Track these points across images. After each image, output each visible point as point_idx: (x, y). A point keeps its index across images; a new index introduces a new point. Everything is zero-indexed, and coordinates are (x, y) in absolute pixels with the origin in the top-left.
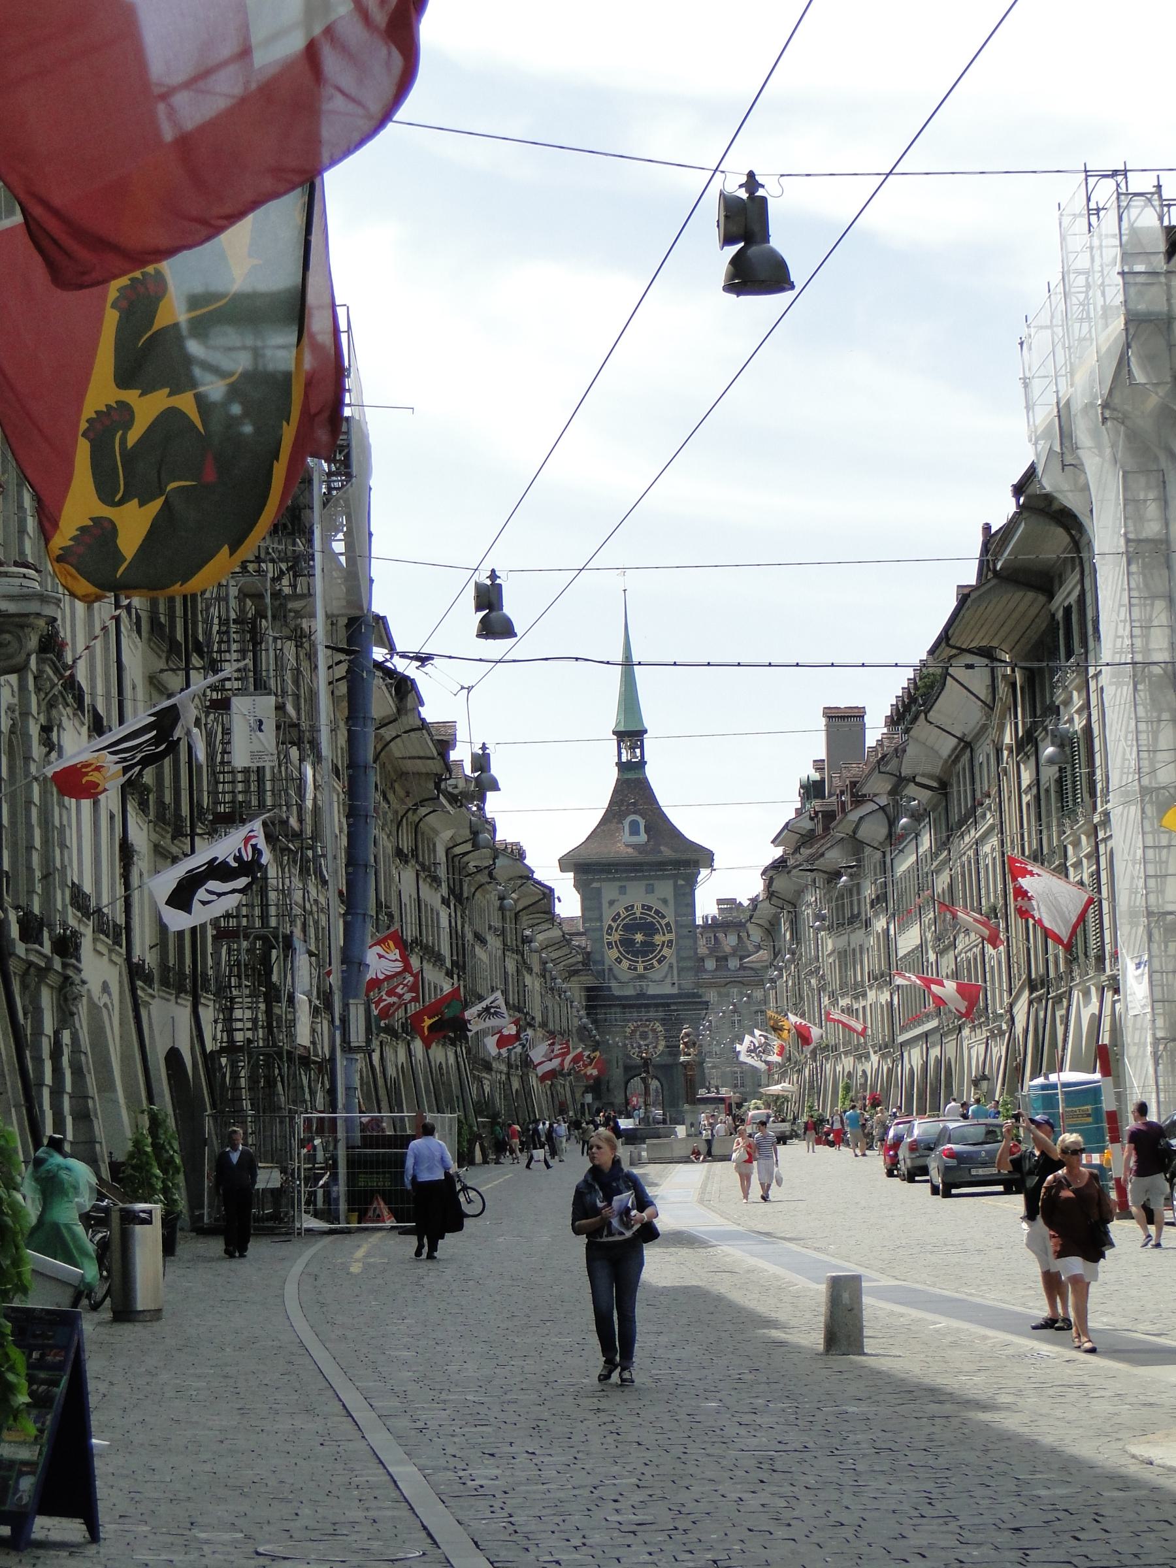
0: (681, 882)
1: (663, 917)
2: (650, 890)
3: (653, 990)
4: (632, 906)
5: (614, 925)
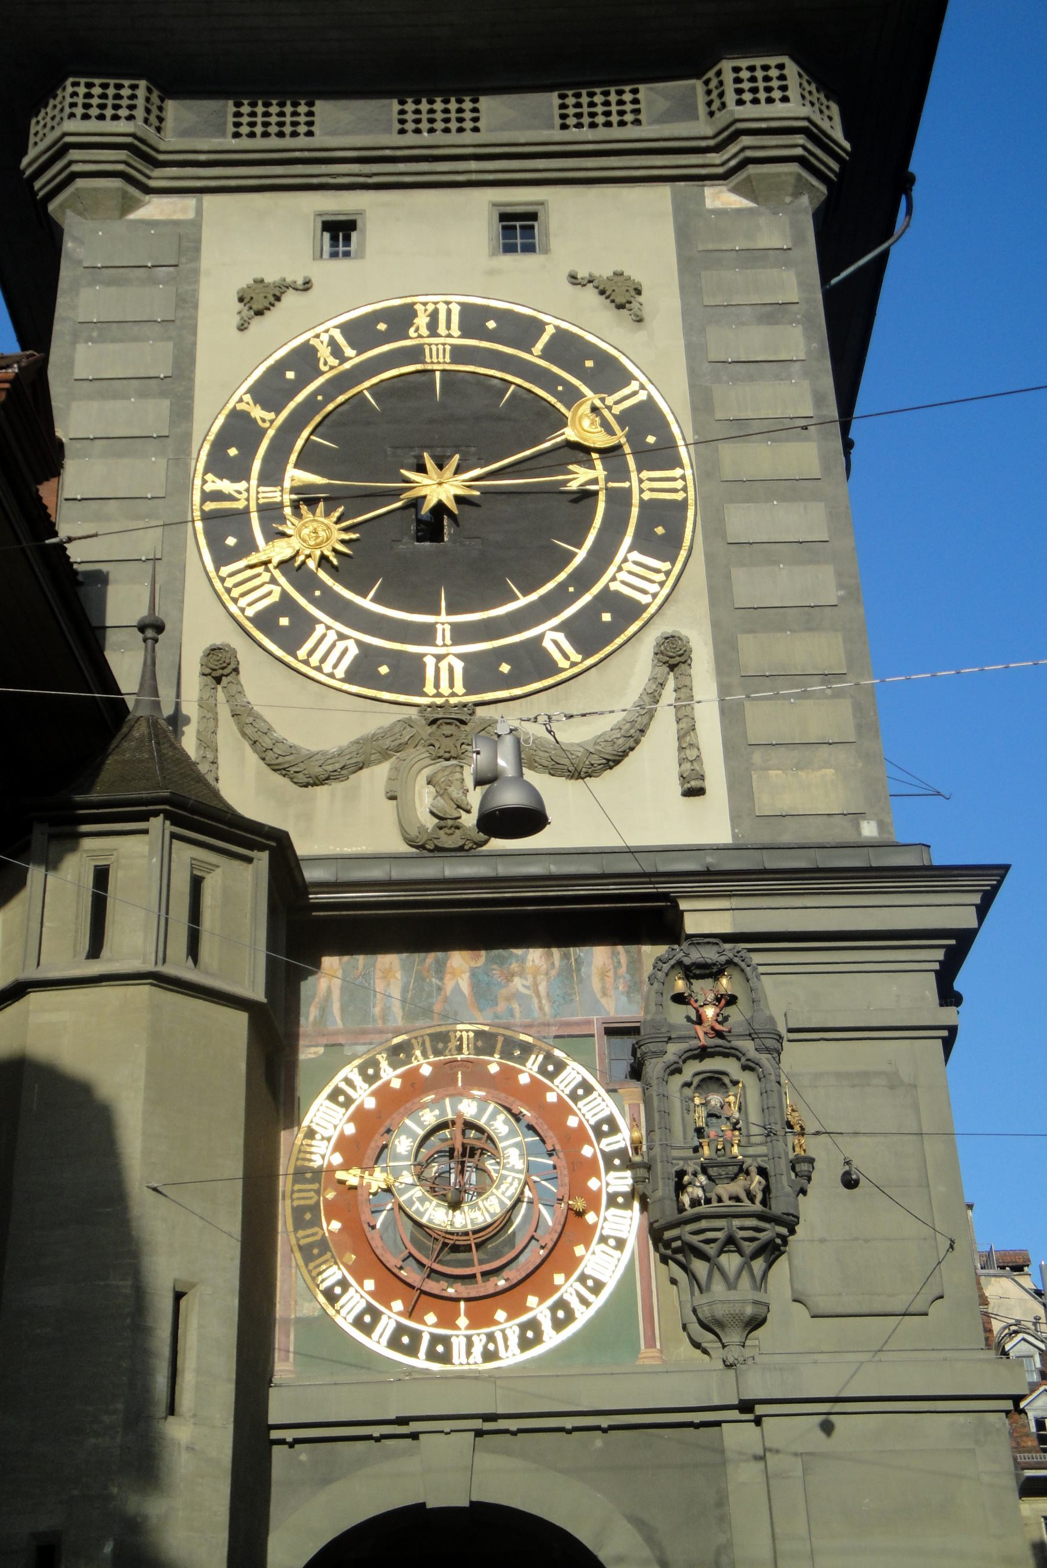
0: (720, 198)
4: (401, 319)
5: (270, 421)
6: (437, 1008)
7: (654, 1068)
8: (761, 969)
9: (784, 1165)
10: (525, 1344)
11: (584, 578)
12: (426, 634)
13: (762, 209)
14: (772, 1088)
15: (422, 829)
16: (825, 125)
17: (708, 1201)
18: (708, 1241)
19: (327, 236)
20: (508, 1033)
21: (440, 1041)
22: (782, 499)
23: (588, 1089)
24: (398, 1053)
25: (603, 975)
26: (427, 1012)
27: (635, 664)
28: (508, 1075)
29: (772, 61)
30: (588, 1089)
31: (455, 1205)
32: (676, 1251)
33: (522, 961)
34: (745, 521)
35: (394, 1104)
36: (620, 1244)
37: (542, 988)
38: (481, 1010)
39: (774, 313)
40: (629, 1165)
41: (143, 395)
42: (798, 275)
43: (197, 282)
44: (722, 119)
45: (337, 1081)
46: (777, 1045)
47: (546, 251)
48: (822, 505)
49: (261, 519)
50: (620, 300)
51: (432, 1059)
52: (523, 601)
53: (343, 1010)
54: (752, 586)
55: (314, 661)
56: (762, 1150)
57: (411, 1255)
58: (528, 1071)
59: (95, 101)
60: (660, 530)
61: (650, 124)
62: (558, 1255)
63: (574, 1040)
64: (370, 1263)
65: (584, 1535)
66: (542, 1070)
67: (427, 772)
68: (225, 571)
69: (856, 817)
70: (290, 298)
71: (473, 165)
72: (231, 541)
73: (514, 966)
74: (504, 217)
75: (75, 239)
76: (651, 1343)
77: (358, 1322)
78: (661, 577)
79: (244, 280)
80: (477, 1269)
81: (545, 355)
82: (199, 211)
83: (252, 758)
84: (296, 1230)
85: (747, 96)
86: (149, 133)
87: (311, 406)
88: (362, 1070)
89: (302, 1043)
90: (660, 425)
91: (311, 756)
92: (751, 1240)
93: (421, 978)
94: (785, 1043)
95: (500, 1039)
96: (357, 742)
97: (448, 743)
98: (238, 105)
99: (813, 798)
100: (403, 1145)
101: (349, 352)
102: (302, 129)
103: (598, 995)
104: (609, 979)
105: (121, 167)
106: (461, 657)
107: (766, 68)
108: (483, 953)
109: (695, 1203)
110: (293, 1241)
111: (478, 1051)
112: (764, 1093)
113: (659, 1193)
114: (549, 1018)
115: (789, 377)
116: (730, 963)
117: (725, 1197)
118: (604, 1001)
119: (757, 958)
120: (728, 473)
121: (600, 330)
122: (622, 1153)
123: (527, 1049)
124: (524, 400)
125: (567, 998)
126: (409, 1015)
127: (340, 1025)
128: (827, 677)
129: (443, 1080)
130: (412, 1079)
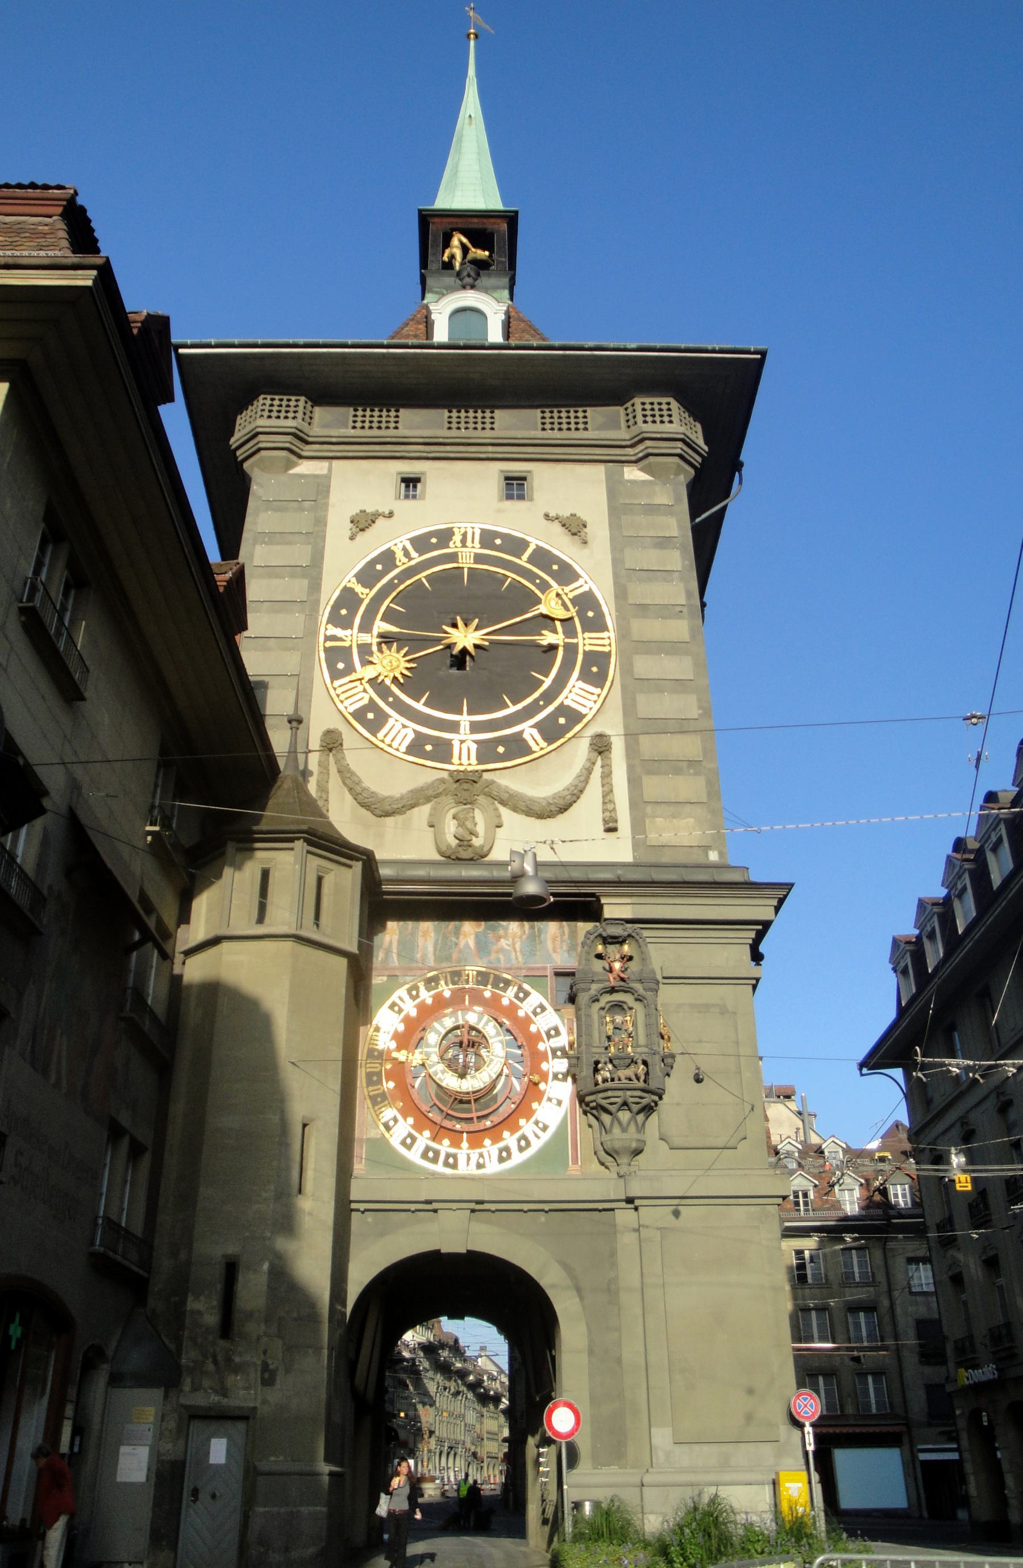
0: (633, 474)
1: (566, 574)
2: (515, 487)
3: (518, 845)
4: (445, 536)
6: (455, 956)
7: (583, 998)
8: (648, 940)
9: (657, 1059)
10: (501, 1160)
11: (549, 696)
12: (454, 727)
13: (657, 481)
14: (652, 1012)
15: (449, 846)
16: (693, 437)
17: (613, 1080)
18: (611, 1104)
19: (403, 485)
20: (497, 973)
21: (456, 976)
22: (667, 653)
23: (543, 1009)
24: (431, 983)
25: (554, 939)
26: (448, 958)
27: (578, 751)
28: (496, 999)
29: (664, 400)
30: (543, 1009)
31: (462, 1076)
32: (592, 1108)
33: (506, 929)
34: (645, 666)
35: (428, 1013)
36: (559, 1103)
37: (518, 946)
38: (481, 958)
39: (663, 543)
40: (565, 1054)
41: (292, 576)
42: (678, 521)
43: (327, 510)
44: (635, 430)
45: (394, 998)
46: (656, 987)
47: (531, 499)
48: (690, 658)
49: (359, 653)
50: (573, 531)
51: (451, 986)
52: (512, 709)
53: (399, 955)
54: (650, 706)
55: (388, 740)
56: (645, 1050)
57: (435, 1104)
58: (508, 996)
59: (275, 408)
60: (595, 669)
61: (593, 430)
62: (523, 1108)
63: (535, 978)
64: (411, 1108)
65: (532, 1271)
66: (517, 997)
67: (453, 811)
68: (337, 683)
69: (706, 848)
70: (380, 522)
71: (490, 449)
72: (341, 666)
73: (501, 932)
74: (507, 478)
75: (259, 484)
76: (575, 1161)
77: (403, 1143)
78: (595, 698)
79: (355, 511)
80: (474, 1115)
81: (530, 561)
82: (330, 469)
83: (349, 798)
84: (367, 1086)
85: (649, 419)
86: (305, 426)
87: (390, 586)
88: (409, 991)
89: (374, 973)
90: (596, 606)
91: (385, 799)
92: (638, 1103)
93: (445, 937)
94: (661, 985)
95: (492, 976)
96: (412, 791)
97: (466, 794)
98: (356, 410)
99: (680, 834)
100: (432, 1038)
101: (414, 554)
102: (392, 425)
103: (551, 951)
104: (558, 942)
105: (287, 445)
106: (475, 742)
107: (660, 404)
108: (483, 923)
109: (605, 1080)
110: (366, 1093)
111: (478, 983)
112: (647, 1016)
113: (584, 1074)
114: (521, 965)
115: (672, 581)
116: (630, 936)
117: (623, 1078)
118: (554, 955)
119: (646, 933)
120: (635, 636)
121: (562, 547)
122: (563, 1049)
123: (508, 983)
124: (515, 585)
125: (532, 953)
126: (438, 959)
127: (396, 964)
128: (692, 763)
129: (457, 1000)
130: (438, 999)
